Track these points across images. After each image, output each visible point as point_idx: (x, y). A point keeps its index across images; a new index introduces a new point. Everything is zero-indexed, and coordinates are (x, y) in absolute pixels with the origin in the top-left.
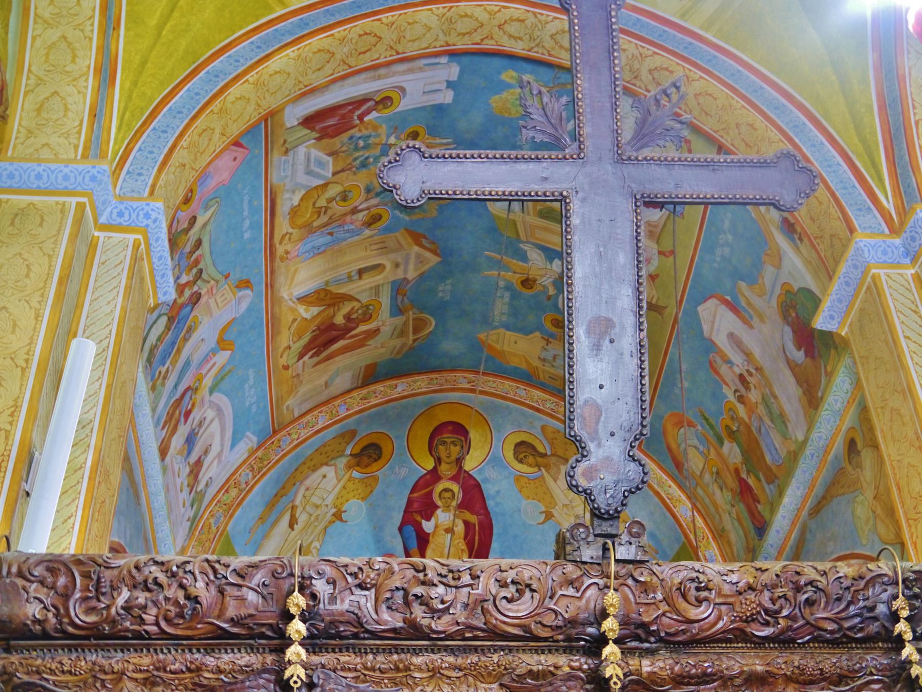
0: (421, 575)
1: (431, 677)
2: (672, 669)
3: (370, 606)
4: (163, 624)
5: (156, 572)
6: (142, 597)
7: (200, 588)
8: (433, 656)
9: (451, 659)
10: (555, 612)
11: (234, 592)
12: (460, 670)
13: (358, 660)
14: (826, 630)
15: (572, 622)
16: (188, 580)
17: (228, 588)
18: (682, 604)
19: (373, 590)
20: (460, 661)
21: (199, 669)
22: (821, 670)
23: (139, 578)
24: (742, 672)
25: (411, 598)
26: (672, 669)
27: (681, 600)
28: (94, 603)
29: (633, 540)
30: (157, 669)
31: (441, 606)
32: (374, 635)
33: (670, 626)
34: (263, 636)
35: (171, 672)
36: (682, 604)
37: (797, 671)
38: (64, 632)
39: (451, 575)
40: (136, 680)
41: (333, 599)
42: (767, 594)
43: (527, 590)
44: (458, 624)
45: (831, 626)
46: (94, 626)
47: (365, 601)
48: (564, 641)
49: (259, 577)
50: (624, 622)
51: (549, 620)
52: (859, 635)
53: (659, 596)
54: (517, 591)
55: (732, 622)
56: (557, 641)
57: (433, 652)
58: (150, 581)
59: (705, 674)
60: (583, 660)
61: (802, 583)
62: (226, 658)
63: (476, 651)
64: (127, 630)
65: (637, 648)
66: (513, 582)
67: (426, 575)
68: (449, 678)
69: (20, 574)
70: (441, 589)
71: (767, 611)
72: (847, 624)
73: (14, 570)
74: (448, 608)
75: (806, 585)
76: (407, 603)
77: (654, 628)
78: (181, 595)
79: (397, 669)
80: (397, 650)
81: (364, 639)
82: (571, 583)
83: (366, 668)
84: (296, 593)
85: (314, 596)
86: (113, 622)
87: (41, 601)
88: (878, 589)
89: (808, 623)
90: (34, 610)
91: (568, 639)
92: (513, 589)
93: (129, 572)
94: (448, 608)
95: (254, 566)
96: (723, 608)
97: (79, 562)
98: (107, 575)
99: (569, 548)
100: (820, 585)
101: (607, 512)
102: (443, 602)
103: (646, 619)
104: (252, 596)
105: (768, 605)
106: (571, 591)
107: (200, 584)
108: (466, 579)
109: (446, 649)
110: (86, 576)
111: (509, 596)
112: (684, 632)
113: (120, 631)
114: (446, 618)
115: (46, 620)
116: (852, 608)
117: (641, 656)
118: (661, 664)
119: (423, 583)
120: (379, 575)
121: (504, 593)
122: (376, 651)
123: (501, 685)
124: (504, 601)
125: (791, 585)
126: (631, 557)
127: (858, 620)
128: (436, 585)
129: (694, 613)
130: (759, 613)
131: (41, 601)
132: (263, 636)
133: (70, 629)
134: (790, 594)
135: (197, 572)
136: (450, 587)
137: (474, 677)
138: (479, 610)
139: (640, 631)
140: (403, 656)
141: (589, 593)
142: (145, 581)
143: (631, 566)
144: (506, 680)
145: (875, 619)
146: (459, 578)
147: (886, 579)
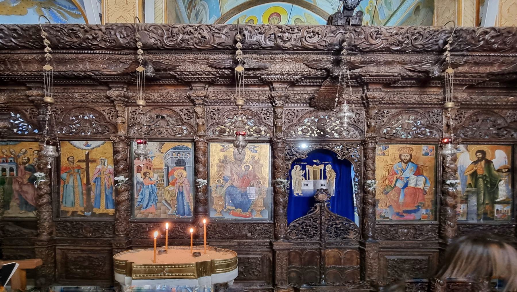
0: (280, 30)
1: (282, 61)
2: (361, 59)
3: (263, 39)
4: (195, 45)
5: (190, 29)
6: (186, 37)
7: (205, 33)
8: (283, 55)
9: (289, 56)
10: (326, 41)
11: (218, 35)
12: (291, 59)
13: (259, 56)
14: (418, 48)
15: (331, 45)
16: (201, 31)
17: (215, 34)
18: (370, 39)
19: (264, 35)
20: (291, 56)
21: (208, 59)
22: (411, 60)
23: (185, 31)
24: (384, 60)
25: (277, 37)
26: (361, 59)
27: (370, 38)
28: (171, 39)
29: (357, 18)
30: (196, 59)
31: (287, 39)
32: (264, 48)
33: (364, 46)
34: (228, 49)
35: (200, 60)
36: (370, 39)
37: (402, 61)
38: (164, 47)
39: (291, 30)
40: (189, 62)
41: (250, 37)
42: (401, 36)
43: (317, 35)
44: (292, 45)
45: (420, 47)
46: (173, 46)
47: (262, 38)
48: (326, 51)
49: (225, 31)
50: (349, 45)
51: (323, 44)
52: (429, 49)
53: (363, 37)
54: (313, 35)
55: (386, 45)
56: (325, 51)
57: (283, 54)
58: (189, 32)
59: (371, 61)
60: (332, 57)
61: (416, 32)
62: (216, 56)
63: (297, 54)
64: (184, 47)
65: (350, 53)
66: (312, 32)
67: (282, 29)
68: (287, 61)
69: (145, 30)
70: (287, 34)
71: (399, 42)
72: (426, 46)
73: (143, 28)
74: (289, 40)
75: (417, 33)
76: (275, 38)
77: (358, 46)
78: (200, 36)
79: (271, 59)
80: (271, 53)
81: (261, 50)
82: (333, 32)
83: (261, 59)
84: (238, 34)
85: (244, 35)
86: (179, 45)
87: (155, 38)
88: (443, 34)
89: (413, 45)
90: (152, 41)
91: (328, 50)
92: (312, 34)
93: (181, 29)
94: (289, 40)
95: (224, 27)
96: (384, 41)
97: (164, 26)
98: (175, 30)
99: (333, 21)
100: (422, 33)
101: (351, 7)
102: (287, 38)
103: (356, 43)
104: (223, 36)
105: (401, 40)
106: (332, 35)
107: (206, 32)
108: (296, 31)
109: (287, 53)
110: (168, 30)
111: (310, 36)
112: (368, 48)
113: (182, 47)
114: (288, 43)
115: (157, 44)
116: (430, 41)
117: (351, 55)
118: (358, 58)
119: (281, 32)
120: (266, 29)
121: (309, 35)
122: (264, 54)
123: (304, 64)
124: (308, 38)
125: (411, 33)
126: (356, 23)
127: (431, 45)
128: (285, 33)
129: (373, 42)
130: (397, 42)
131: (155, 38)
132: (228, 49)
133: (166, 47)
134: (410, 36)
135: (204, 29)
136: (291, 33)
137: (296, 61)
138: (300, 41)
139: (353, 48)
140: (273, 55)
141: (338, 35)
142: (187, 32)
143: (354, 27)
144: (306, 62)
145: (437, 44)
146: (294, 31)
147: (447, 32)
